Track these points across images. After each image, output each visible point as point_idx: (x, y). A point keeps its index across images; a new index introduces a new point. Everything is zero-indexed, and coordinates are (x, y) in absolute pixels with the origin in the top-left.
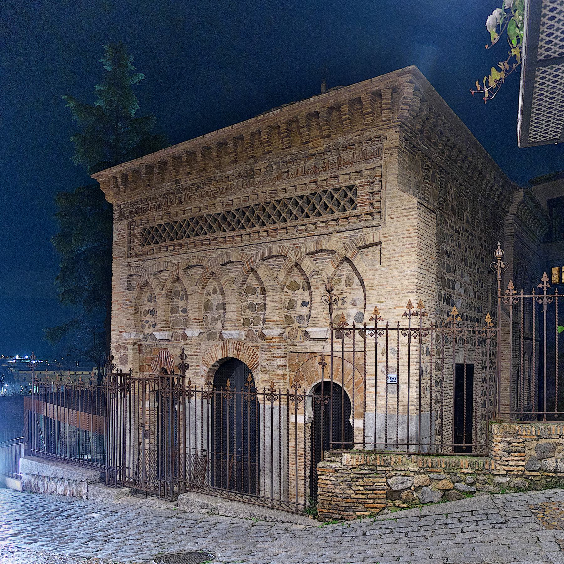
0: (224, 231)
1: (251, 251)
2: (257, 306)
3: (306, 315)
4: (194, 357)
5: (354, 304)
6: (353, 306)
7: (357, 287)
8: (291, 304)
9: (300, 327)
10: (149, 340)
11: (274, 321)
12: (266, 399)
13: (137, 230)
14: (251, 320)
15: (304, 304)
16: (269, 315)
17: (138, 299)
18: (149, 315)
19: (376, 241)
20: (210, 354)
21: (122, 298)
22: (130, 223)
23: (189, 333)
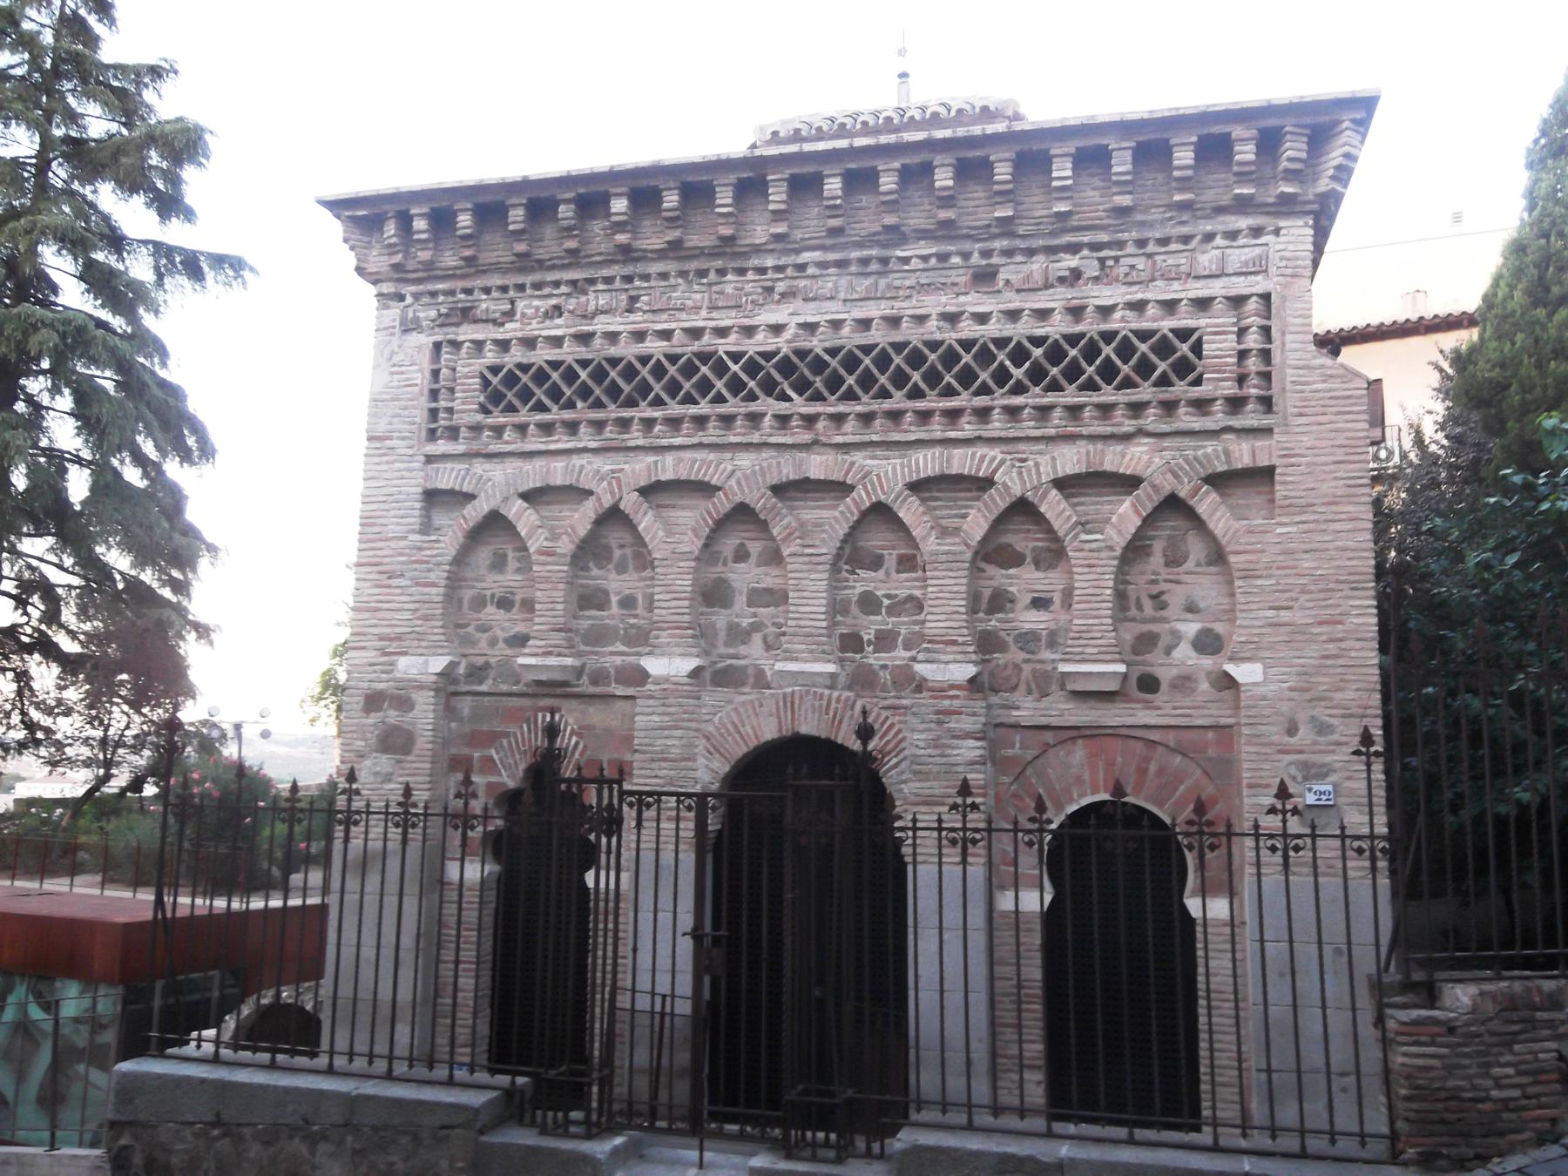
0: (785, 398)
1: (873, 458)
2: (886, 602)
3: (1044, 633)
4: (678, 733)
5: (1191, 608)
6: (1190, 616)
7: (1199, 569)
8: (1000, 602)
9: (1027, 661)
10: (490, 682)
11: (954, 643)
12: (945, 842)
13: (469, 368)
14: (866, 638)
15: (1039, 603)
16: (935, 624)
17: (460, 559)
18: (490, 609)
19: (1263, 462)
20: (736, 727)
21: (401, 555)
22: (437, 346)
23: (655, 666)
